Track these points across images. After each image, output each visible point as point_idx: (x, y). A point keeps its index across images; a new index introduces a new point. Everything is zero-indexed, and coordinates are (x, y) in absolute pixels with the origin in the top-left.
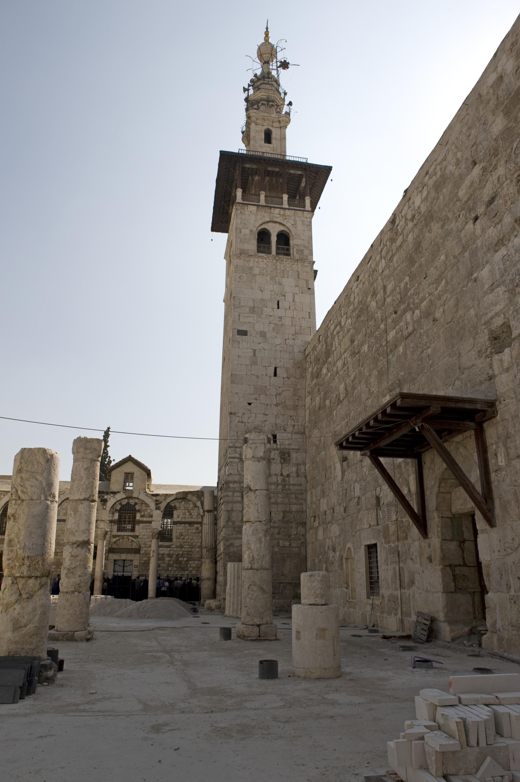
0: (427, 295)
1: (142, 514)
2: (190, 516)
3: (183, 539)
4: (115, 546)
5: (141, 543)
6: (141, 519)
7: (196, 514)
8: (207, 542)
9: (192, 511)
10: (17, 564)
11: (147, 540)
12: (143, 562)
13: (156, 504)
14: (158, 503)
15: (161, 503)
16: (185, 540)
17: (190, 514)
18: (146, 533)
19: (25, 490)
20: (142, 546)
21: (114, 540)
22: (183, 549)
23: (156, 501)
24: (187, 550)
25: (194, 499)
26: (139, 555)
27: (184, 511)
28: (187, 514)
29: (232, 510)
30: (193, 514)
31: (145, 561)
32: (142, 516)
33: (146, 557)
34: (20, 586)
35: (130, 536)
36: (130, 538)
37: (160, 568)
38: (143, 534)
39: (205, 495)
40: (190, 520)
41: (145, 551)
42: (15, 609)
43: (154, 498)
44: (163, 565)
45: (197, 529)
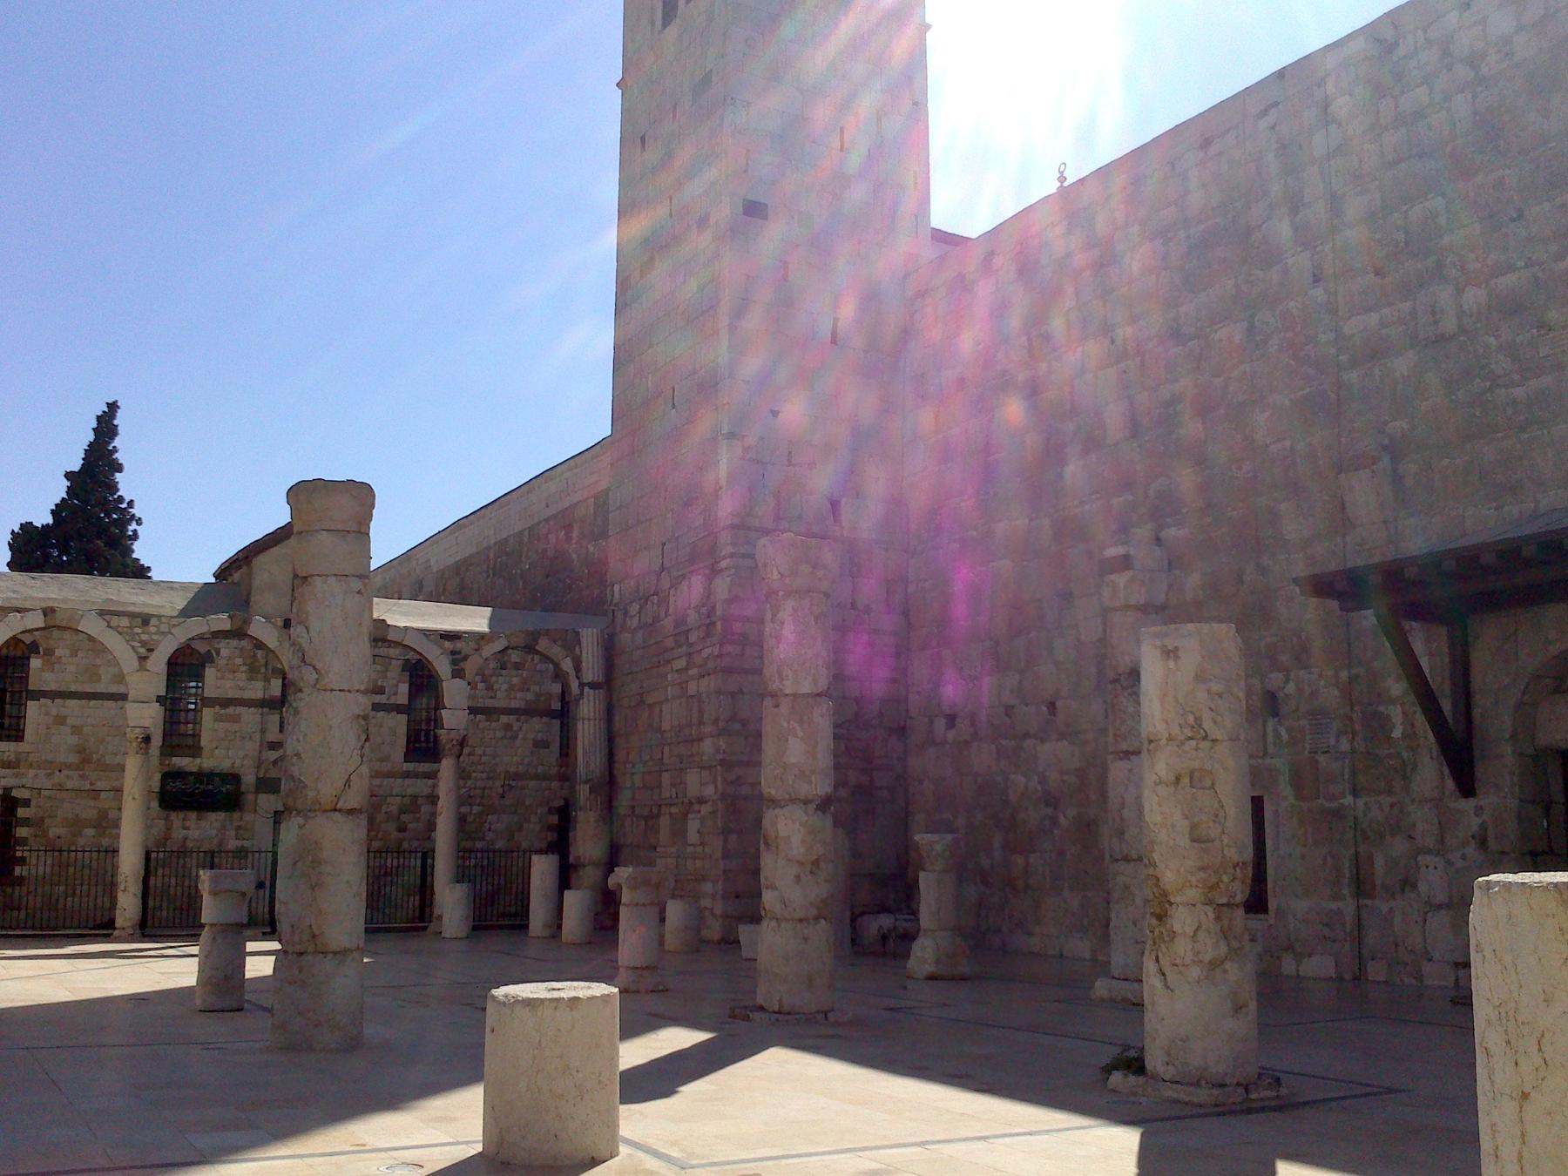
0: (1521, 264)
4: (273, 774)
7: (504, 687)
8: (592, 766)
10: (1225, 879)
13: (454, 663)
14: (457, 659)
15: (465, 658)
16: (475, 759)
17: (490, 688)
19: (1219, 719)
21: (273, 755)
22: (469, 783)
23: (453, 653)
24: (479, 784)
25: (556, 651)
28: (480, 686)
29: (741, 692)
34: (1226, 922)
39: (584, 643)
40: (490, 703)
42: (1225, 971)
43: (447, 644)
45: (508, 727)
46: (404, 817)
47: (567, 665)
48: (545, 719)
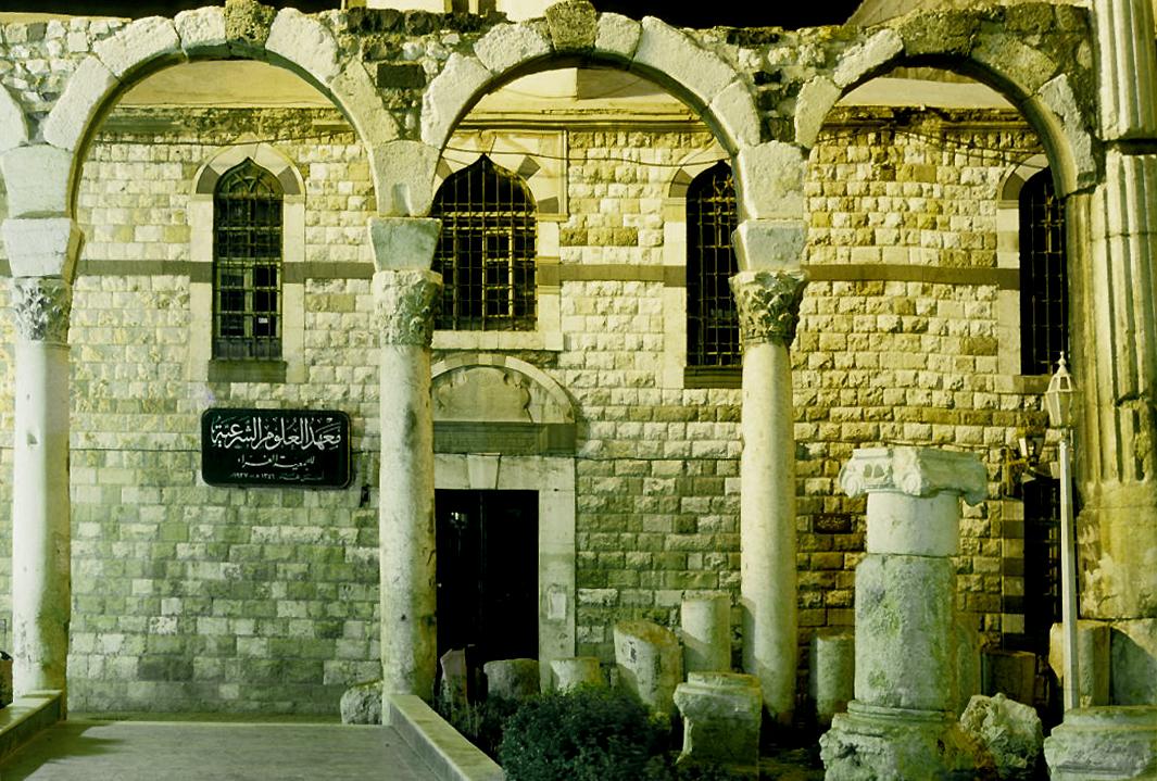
1: (573, 223)
2: (861, 234)
3: (822, 368)
5: (578, 395)
6: (568, 254)
7: (893, 219)
9: (868, 202)
11: (612, 378)
12: (595, 502)
13: (764, 103)
18: (602, 340)
20: (590, 411)
22: (827, 428)
26: (567, 464)
27: (816, 203)
28: (839, 218)
30: (874, 218)
31: (610, 498)
32: (569, 240)
33: (612, 473)
35: (513, 352)
36: (512, 362)
37: (698, 539)
38: (587, 342)
40: (863, 256)
41: (605, 442)
44: (711, 520)
46: (692, 503)
47: (1055, 98)
48: (984, 291)
